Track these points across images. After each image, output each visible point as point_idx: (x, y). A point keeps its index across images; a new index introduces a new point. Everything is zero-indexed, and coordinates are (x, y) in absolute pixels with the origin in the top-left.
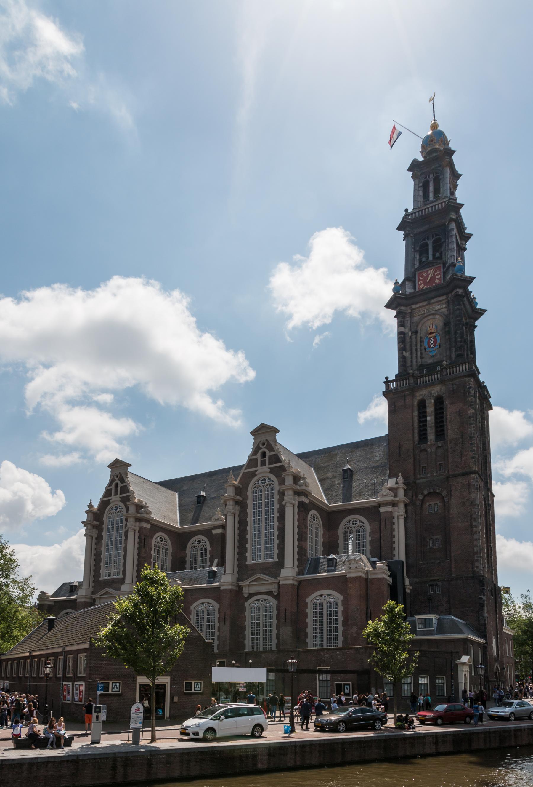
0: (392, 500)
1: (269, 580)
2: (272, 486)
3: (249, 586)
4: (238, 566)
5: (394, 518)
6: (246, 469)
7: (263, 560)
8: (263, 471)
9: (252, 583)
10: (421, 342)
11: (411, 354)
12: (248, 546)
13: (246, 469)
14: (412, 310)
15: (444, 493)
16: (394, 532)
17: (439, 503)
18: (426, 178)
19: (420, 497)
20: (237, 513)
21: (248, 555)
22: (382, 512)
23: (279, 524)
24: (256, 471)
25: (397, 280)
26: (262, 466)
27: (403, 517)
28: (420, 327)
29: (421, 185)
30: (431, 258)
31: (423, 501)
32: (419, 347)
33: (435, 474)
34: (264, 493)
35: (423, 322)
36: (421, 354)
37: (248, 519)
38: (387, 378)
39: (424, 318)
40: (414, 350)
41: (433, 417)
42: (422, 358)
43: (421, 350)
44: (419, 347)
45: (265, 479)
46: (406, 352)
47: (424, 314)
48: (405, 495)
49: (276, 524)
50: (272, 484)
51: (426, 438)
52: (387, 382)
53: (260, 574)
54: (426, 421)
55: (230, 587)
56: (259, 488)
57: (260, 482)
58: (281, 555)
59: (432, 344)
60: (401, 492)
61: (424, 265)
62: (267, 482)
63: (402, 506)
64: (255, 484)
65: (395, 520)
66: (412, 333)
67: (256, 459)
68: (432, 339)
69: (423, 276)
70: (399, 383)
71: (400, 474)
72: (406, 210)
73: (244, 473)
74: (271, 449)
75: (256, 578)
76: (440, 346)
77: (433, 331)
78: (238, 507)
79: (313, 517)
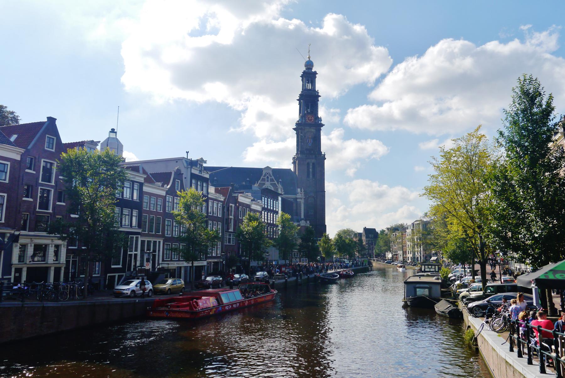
15: (315, 197)
31: (308, 198)
54: (309, 170)
60: (303, 194)
63: (303, 199)
67: (265, 179)
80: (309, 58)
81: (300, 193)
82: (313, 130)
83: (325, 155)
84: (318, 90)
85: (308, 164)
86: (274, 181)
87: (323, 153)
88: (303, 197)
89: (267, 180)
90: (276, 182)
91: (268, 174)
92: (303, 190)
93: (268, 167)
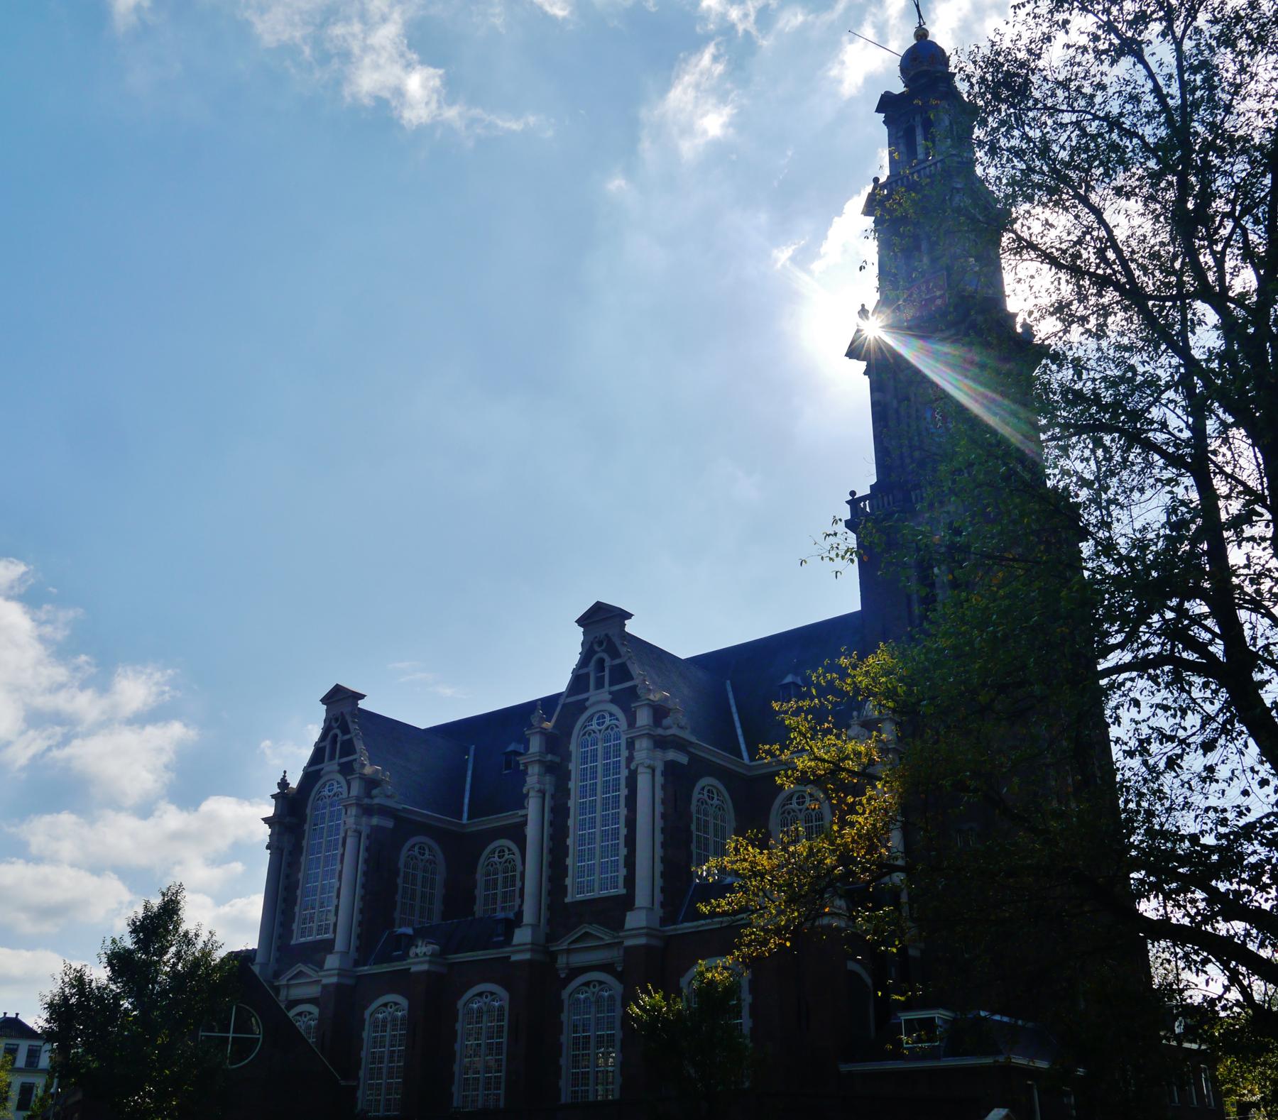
1: (607, 938)
2: (615, 729)
3: (568, 951)
4: (550, 907)
6: (567, 697)
8: (599, 698)
9: (573, 946)
12: (569, 861)
13: (567, 697)
18: (909, 121)
20: (549, 789)
21: (568, 881)
24: (587, 699)
25: (863, 306)
29: (901, 134)
34: (600, 747)
37: (571, 803)
45: (604, 717)
49: (623, 811)
50: (617, 727)
52: (854, 502)
53: (590, 924)
55: (527, 956)
56: (593, 735)
57: (595, 721)
58: (630, 881)
62: (607, 723)
64: (586, 727)
67: (588, 675)
72: (876, 180)
73: (564, 706)
74: (614, 653)
75: (579, 934)
78: (548, 778)
79: (709, 791)
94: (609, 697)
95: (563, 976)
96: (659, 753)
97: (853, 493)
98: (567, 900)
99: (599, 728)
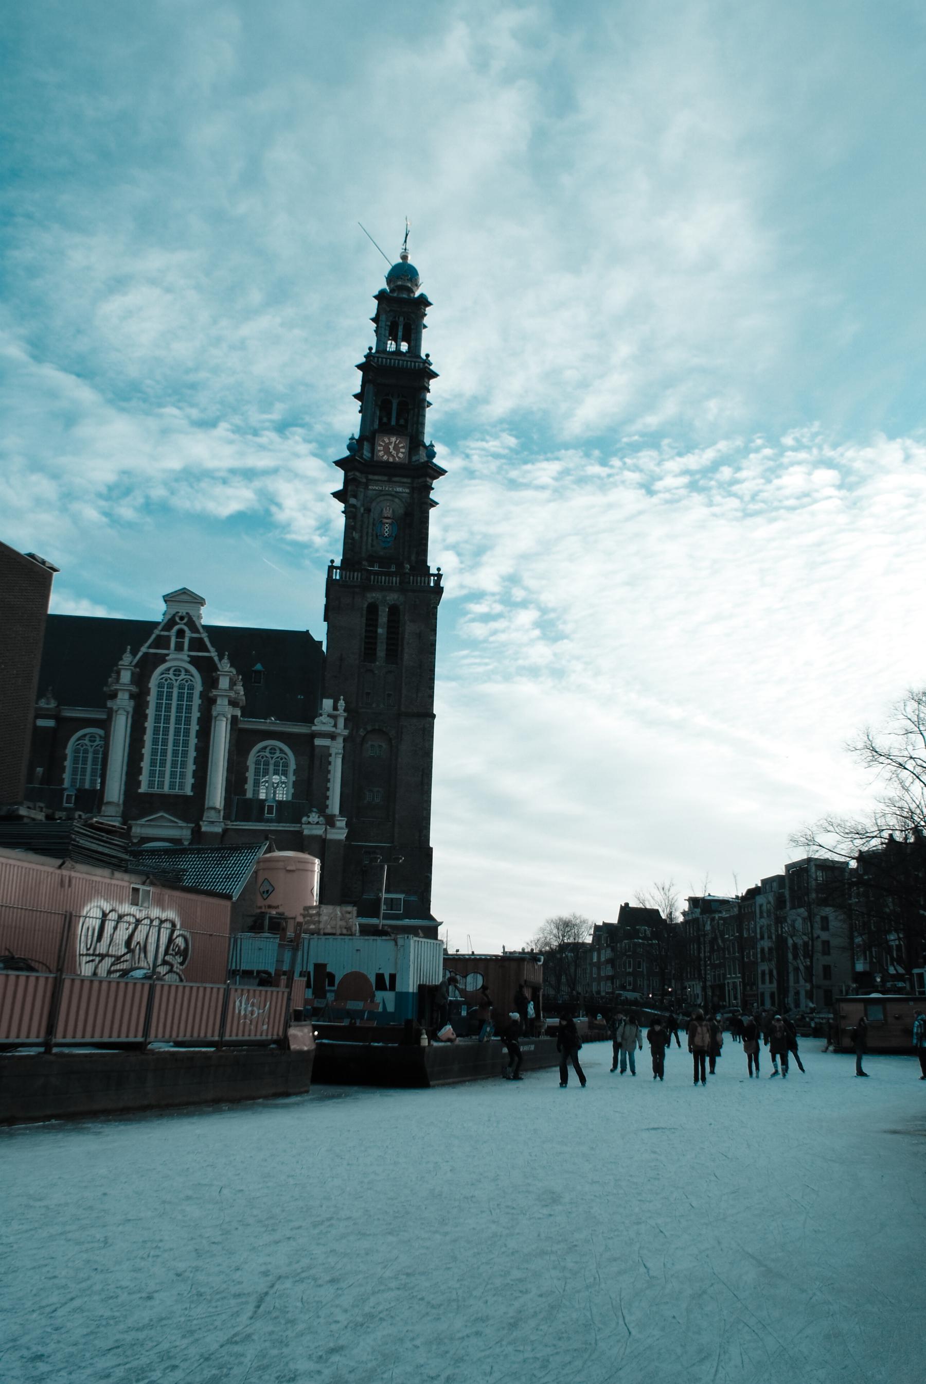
0: (334, 732)
2: (189, 682)
5: (330, 755)
7: (166, 789)
10: (374, 525)
11: (361, 537)
13: (149, 647)
14: (368, 480)
16: (329, 775)
17: (384, 745)
18: (395, 317)
19: (362, 732)
22: (317, 746)
23: (198, 741)
26: (176, 650)
27: (341, 756)
28: (374, 504)
29: (389, 323)
30: (393, 422)
31: (364, 737)
32: (370, 531)
33: (382, 706)
35: (378, 500)
36: (372, 540)
38: (332, 561)
39: (381, 496)
40: (365, 534)
41: (385, 630)
42: (372, 546)
43: (372, 535)
44: (370, 531)
45: (180, 671)
46: (356, 533)
47: (382, 491)
48: (345, 727)
50: (191, 681)
51: (375, 654)
54: (376, 631)
57: (171, 672)
59: (386, 532)
60: (341, 722)
61: (386, 429)
63: (340, 740)
65: (331, 759)
66: (364, 510)
67: (169, 638)
68: (387, 525)
69: (384, 441)
70: (344, 572)
71: (342, 697)
72: (370, 349)
73: (146, 654)
76: (395, 538)
77: (389, 516)
80: (404, 258)
81: (329, 716)
82: (399, 489)
83: (439, 576)
84: (427, 356)
85: (373, 610)
86: (208, 651)
87: (433, 571)
88: (341, 729)
89: (177, 643)
90: (213, 654)
91: (182, 618)
92: (342, 704)
93: (184, 591)
94: (188, 659)
95: (135, 841)
96: (231, 708)
97: (332, 561)
98: (140, 791)
99: (176, 678)
